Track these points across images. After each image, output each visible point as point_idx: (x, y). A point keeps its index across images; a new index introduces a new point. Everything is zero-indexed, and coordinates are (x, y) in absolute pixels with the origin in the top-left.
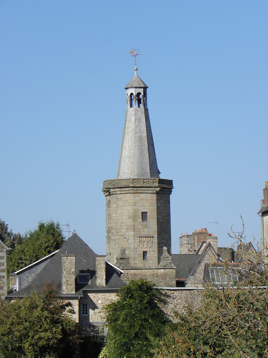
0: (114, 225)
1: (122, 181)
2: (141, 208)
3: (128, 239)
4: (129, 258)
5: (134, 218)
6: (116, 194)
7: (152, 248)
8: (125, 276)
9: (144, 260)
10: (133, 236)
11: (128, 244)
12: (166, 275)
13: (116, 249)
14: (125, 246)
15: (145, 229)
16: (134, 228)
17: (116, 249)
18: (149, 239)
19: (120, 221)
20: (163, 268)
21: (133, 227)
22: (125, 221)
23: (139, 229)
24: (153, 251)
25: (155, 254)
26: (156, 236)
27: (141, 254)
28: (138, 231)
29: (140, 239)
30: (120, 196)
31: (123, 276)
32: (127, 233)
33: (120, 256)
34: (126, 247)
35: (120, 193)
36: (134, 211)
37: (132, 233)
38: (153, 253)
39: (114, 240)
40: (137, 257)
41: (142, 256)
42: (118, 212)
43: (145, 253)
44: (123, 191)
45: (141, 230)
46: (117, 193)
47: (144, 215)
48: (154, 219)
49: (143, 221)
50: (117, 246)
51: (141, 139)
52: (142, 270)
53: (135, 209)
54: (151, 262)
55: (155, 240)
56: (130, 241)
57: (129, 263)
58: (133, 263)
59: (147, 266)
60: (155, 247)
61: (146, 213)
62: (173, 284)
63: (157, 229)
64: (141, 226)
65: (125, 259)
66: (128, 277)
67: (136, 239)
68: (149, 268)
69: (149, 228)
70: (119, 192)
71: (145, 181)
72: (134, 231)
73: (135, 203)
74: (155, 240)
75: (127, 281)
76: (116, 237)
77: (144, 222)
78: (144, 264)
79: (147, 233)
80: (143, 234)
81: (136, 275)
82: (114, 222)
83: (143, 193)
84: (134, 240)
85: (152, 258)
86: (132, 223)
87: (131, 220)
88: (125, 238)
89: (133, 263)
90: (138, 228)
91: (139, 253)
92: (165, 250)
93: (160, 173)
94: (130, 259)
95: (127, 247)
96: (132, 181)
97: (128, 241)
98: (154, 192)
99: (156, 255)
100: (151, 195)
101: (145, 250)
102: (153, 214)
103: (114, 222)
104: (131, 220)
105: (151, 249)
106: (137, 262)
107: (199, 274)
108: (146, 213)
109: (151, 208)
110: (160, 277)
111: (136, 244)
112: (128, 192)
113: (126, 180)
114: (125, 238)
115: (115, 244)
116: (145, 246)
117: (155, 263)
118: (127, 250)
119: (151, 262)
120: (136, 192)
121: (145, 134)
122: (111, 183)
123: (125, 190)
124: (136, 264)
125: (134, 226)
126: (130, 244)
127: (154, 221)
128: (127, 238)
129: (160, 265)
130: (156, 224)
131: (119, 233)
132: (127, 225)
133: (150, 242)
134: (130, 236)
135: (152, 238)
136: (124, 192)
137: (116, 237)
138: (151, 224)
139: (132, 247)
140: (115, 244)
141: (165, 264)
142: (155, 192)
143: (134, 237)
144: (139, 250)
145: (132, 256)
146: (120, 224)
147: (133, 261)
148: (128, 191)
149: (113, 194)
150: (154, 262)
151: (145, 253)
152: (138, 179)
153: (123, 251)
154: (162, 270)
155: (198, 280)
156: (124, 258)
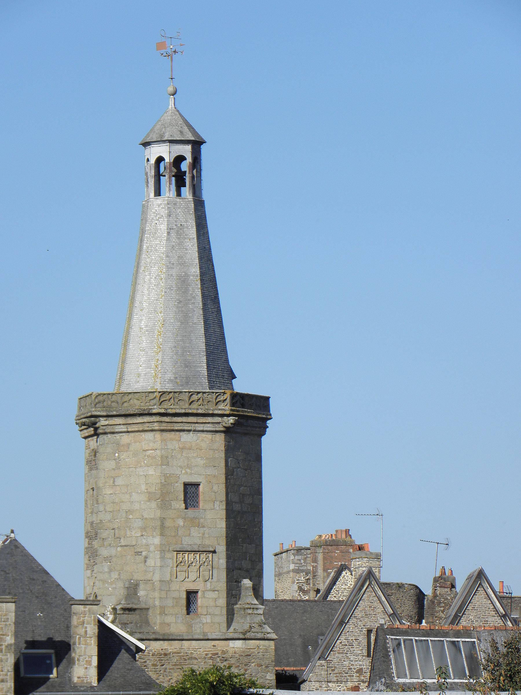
0: (108, 517)
1: (130, 396)
2: (183, 472)
3: (146, 557)
5: (163, 499)
6: (113, 433)
7: (211, 582)
9: (188, 613)
10: (159, 549)
11: (146, 571)
12: (249, 657)
13: (112, 583)
14: (137, 576)
15: (192, 530)
16: (163, 527)
17: (112, 583)
18: (203, 556)
19: (125, 507)
20: (241, 636)
21: (159, 523)
22: (137, 506)
23: (177, 528)
24: (214, 591)
25: (219, 597)
26: (222, 549)
27: (180, 598)
28: (173, 534)
29: (180, 555)
30: (125, 439)
32: (144, 541)
33: (124, 604)
34: (139, 578)
35: (126, 430)
36: (163, 481)
37: (157, 540)
38: (215, 595)
39: (108, 559)
40: (171, 605)
41: (184, 602)
42: (119, 481)
43: (191, 596)
44: (134, 426)
45: (180, 533)
46: (117, 430)
47: (191, 491)
48: (218, 503)
49: (186, 508)
50: (115, 575)
51: (183, 281)
52: (184, 642)
53: (165, 475)
54: (208, 619)
55: (221, 560)
56: (151, 562)
57: (147, 623)
58: (158, 622)
59: (198, 631)
60: (218, 581)
61: (197, 485)
62: (268, 681)
63: (225, 530)
64: (181, 522)
65: (137, 612)
66: (145, 662)
67: (168, 555)
68: (202, 637)
69: (203, 527)
70: (122, 426)
71: (195, 397)
72: (162, 535)
73: (167, 457)
74: (219, 559)
76: (113, 551)
77: (190, 512)
78: (191, 626)
79: (198, 542)
80: (187, 542)
81: (165, 655)
82: (108, 508)
83: (189, 431)
84: (162, 558)
85: (210, 610)
86: (158, 513)
87: (154, 505)
88: (139, 553)
89: (158, 622)
90: (174, 527)
91: (176, 595)
92: (247, 588)
93: (234, 377)
94: (150, 612)
95: (142, 578)
96: (158, 398)
97: (145, 561)
98: (217, 429)
99: (222, 601)
100: (209, 436)
101: (192, 587)
102: (215, 488)
103: (108, 508)
104: (154, 505)
105: (208, 584)
106: (169, 619)
107: (340, 656)
108: (197, 485)
109: (210, 471)
110: (233, 661)
111: (169, 569)
112: (147, 429)
113: (144, 395)
114: (139, 553)
115: (110, 571)
116: (193, 576)
117: (219, 624)
118: (142, 586)
119: (209, 620)
120: (169, 428)
121: (195, 270)
122: (99, 402)
123: (138, 422)
124: (168, 625)
125: (163, 520)
127: (218, 508)
128: (144, 554)
129: (231, 629)
130: (224, 516)
131: (122, 540)
132: (143, 518)
133: (206, 564)
134: (152, 548)
135: (210, 555)
137: (113, 551)
138: (209, 515)
139: (157, 577)
140: (110, 571)
141: (246, 627)
142: (223, 429)
143: (162, 551)
144: (174, 586)
145: (157, 603)
146: (124, 515)
147: (158, 617)
148: (147, 425)
149: (105, 433)
150: (217, 619)
151: (191, 596)
152: (175, 392)
153: (132, 589)
154: (238, 644)
155: (336, 671)
156: (135, 610)
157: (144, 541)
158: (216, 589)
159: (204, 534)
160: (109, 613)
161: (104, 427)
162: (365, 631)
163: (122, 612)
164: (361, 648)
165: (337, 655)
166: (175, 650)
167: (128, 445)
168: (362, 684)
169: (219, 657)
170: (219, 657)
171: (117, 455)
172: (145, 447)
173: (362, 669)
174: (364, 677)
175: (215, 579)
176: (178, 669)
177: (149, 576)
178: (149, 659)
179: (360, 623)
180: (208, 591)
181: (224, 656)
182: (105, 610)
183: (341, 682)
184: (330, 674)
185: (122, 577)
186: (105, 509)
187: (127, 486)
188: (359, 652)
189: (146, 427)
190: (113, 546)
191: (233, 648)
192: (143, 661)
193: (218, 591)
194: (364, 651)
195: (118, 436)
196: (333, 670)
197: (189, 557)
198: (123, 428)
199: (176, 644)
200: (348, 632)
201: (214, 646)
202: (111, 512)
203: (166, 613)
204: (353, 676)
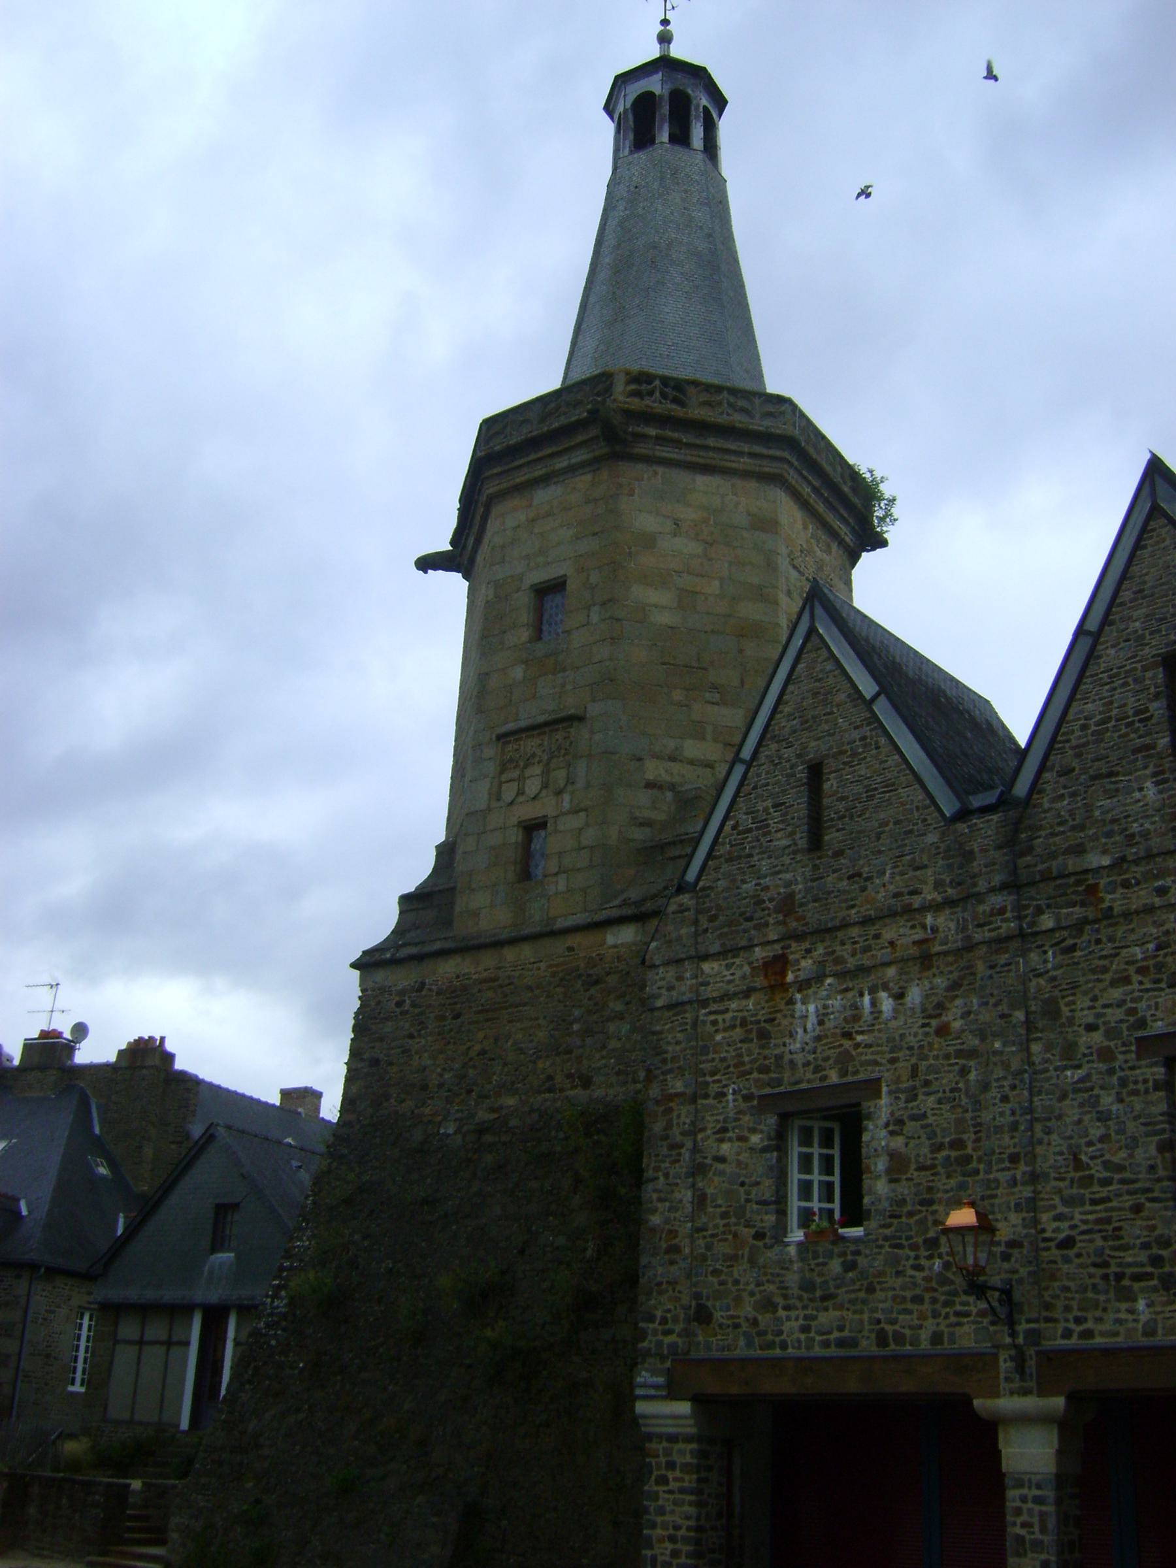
8: (407, 1006)
31: (398, 1004)
74: (592, 733)
75: (411, 1036)
102: (594, 578)
105: (566, 797)
106: (480, 900)
116: (532, 787)
158: (582, 805)
159: (563, 686)
162: (801, 772)
164: (790, 829)
165: (725, 868)
166: (485, 975)
168: (794, 945)
169: (580, 976)
170: (580, 976)
173: (791, 896)
174: (797, 920)
175: (580, 784)
176: (487, 1020)
178: (430, 1006)
179: (787, 753)
180: (564, 814)
181: (591, 972)
183: (735, 951)
184: (706, 931)
188: (784, 842)
191: (615, 946)
192: (417, 1011)
193: (586, 810)
194: (798, 836)
196: (713, 919)
197: (530, 745)
199: (488, 960)
200: (755, 788)
201: (570, 949)
203: (474, 886)
204: (767, 925)
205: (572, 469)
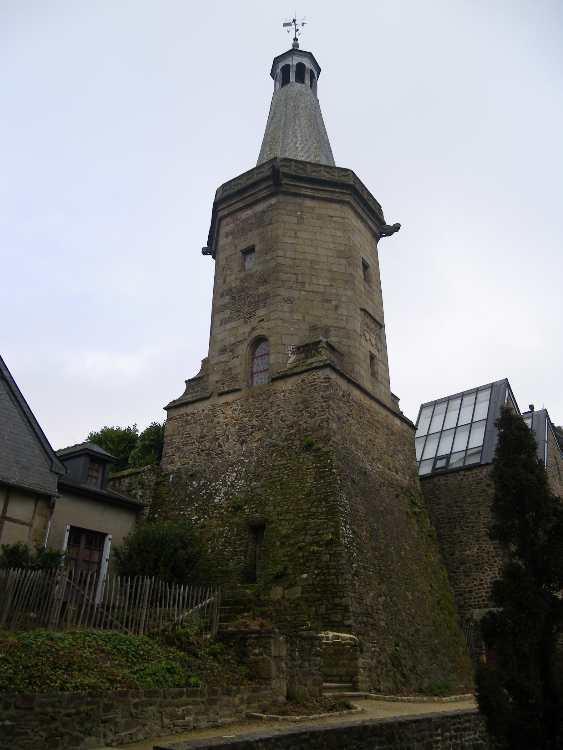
0: (290, 263)
4: (343, 355)
6: (295, 195)
14: (325, 322)
22: (324, 259)
30: (309, 203)
32: (334, 291)
34: (329, 324)
35: (312, 194)
50: (297, 317)
65: (336, 353)
76: (296, 294)
95: (333, 325)
103: (289, 255)
112: (337, 198)
114: (330, 302)
118: (333, 332)
126: (344, 318)
131: (307, 285)
132: (331, 271)
134: (343, 299)
136: (323, 195)
140: (292, 312)
146: (309, 265)
148: (337, 195)
149: (287, 193)
157: (334, 291)
160: (290, 352)
161: (288, 187)
163: (325, 346)
167: (313, 208)
171: (299, 213)
172: (332, 214)
177: (342, 324)
182: (285, 349)
185: (307, 320)
186: (285, 255)
187: (312, 240)
189: (335, 197)
190: (295, 289)
195: (300, 200)
198: (310, 193)
202: (292, 259)
205: (369, 228)
